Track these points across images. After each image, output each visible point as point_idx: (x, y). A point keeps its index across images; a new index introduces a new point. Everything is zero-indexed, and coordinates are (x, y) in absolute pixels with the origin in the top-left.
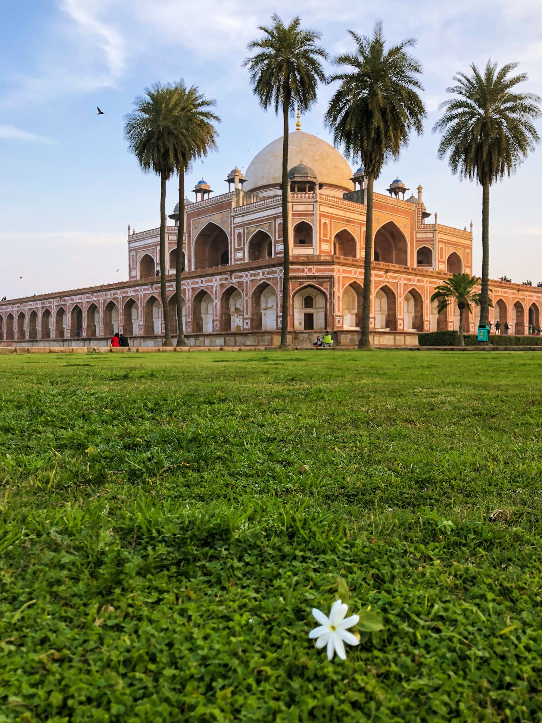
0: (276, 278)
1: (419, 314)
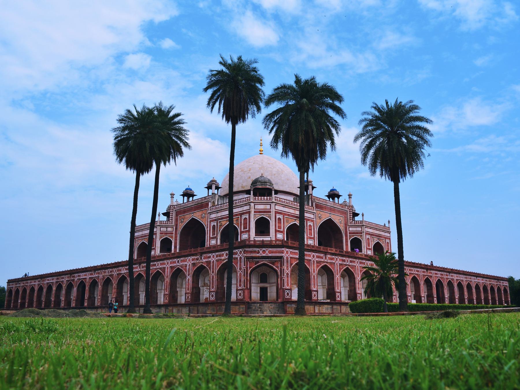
1: (353, 288)
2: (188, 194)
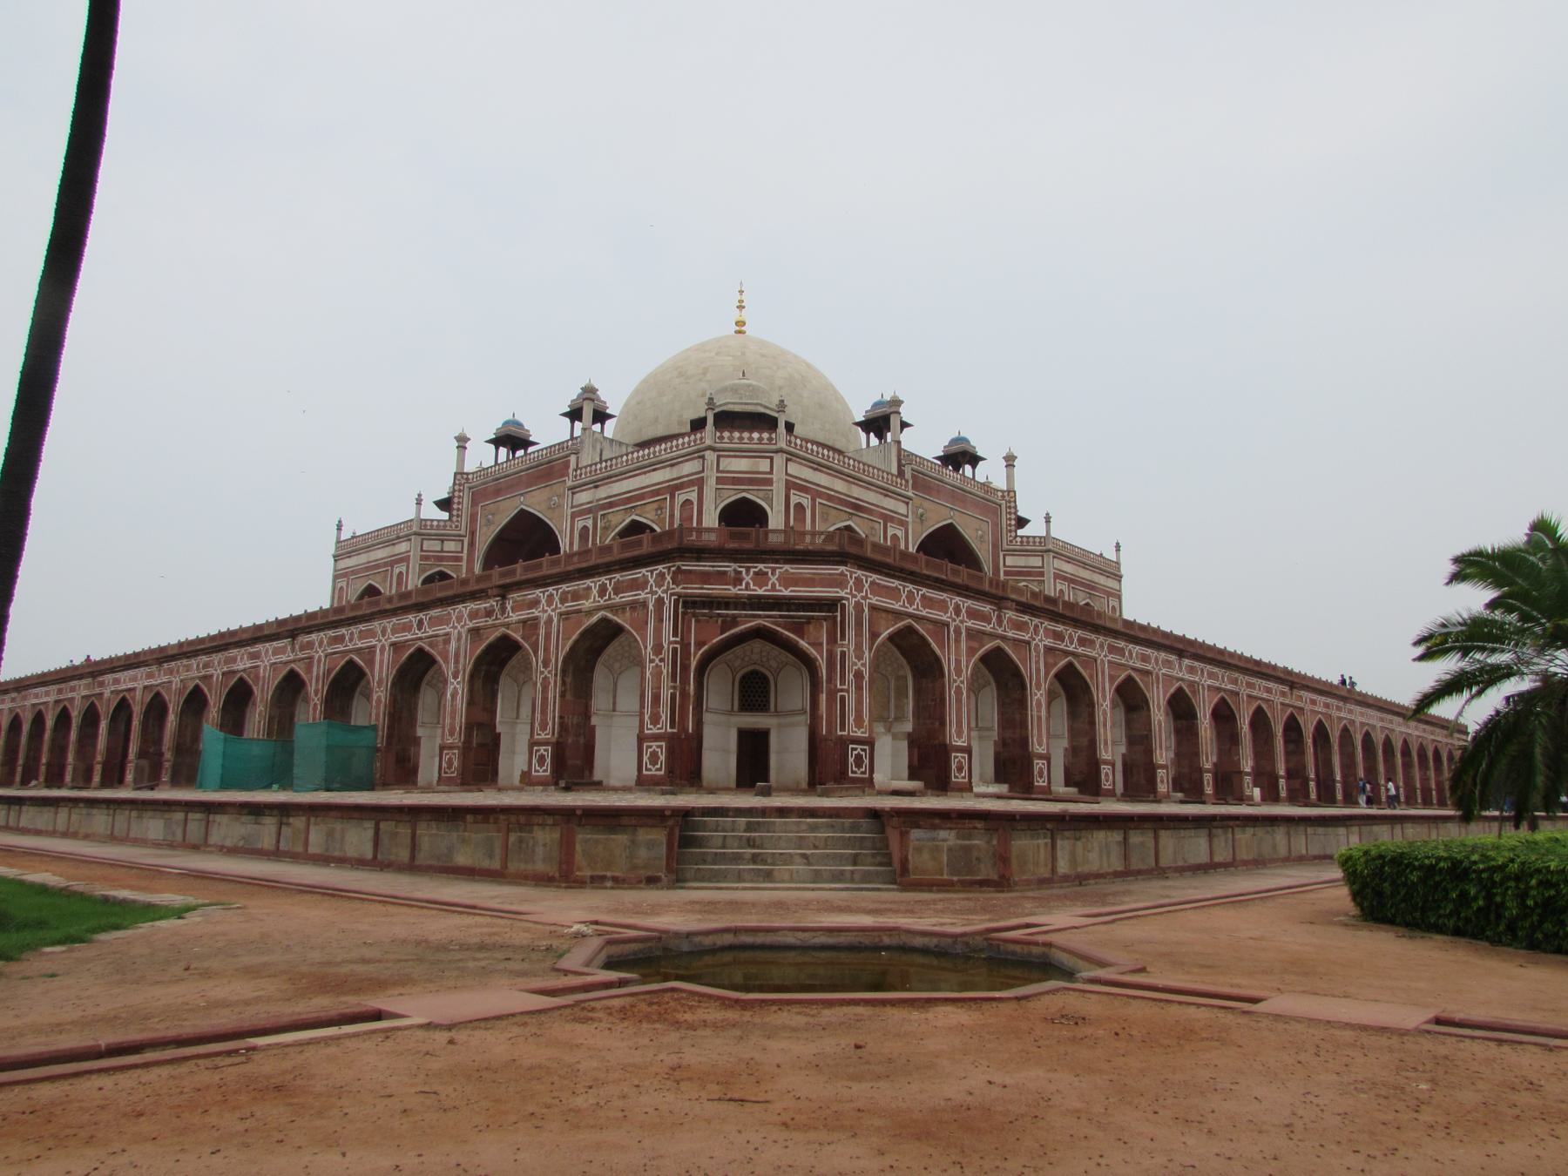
0: (644, 604)
1: (1085, 741)
2: (511, 439)
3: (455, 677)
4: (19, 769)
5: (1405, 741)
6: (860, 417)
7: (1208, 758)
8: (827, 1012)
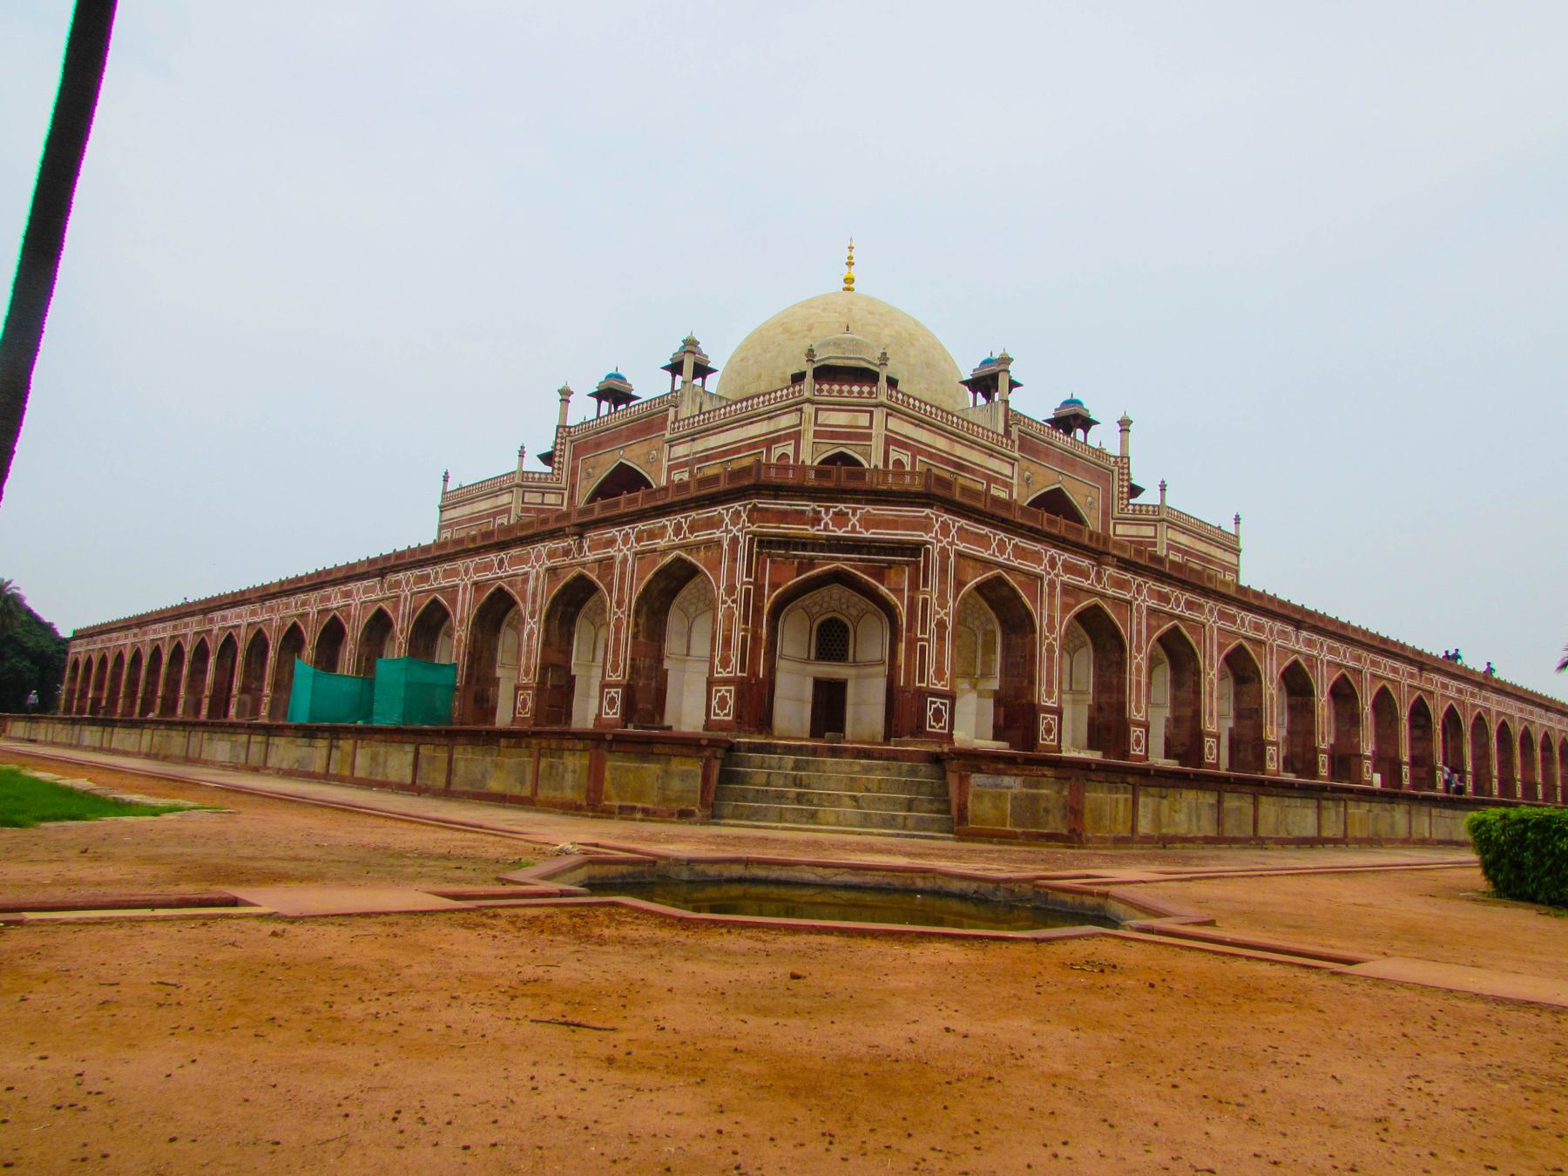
0: (719, 543)
1: (1188, 711)
2: (614, 393)
3: (532, 617)
4: (139, 702)
5: (1546, 735)
6: (967, 377)
7: (1325, 738)
8: (788, 939)
